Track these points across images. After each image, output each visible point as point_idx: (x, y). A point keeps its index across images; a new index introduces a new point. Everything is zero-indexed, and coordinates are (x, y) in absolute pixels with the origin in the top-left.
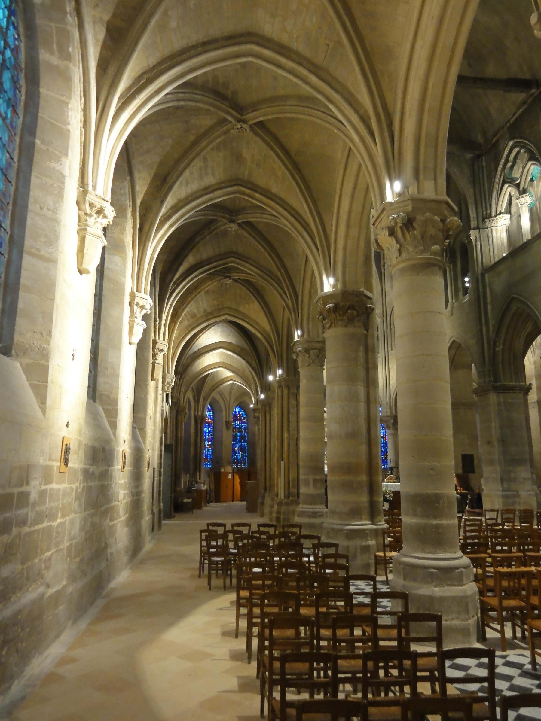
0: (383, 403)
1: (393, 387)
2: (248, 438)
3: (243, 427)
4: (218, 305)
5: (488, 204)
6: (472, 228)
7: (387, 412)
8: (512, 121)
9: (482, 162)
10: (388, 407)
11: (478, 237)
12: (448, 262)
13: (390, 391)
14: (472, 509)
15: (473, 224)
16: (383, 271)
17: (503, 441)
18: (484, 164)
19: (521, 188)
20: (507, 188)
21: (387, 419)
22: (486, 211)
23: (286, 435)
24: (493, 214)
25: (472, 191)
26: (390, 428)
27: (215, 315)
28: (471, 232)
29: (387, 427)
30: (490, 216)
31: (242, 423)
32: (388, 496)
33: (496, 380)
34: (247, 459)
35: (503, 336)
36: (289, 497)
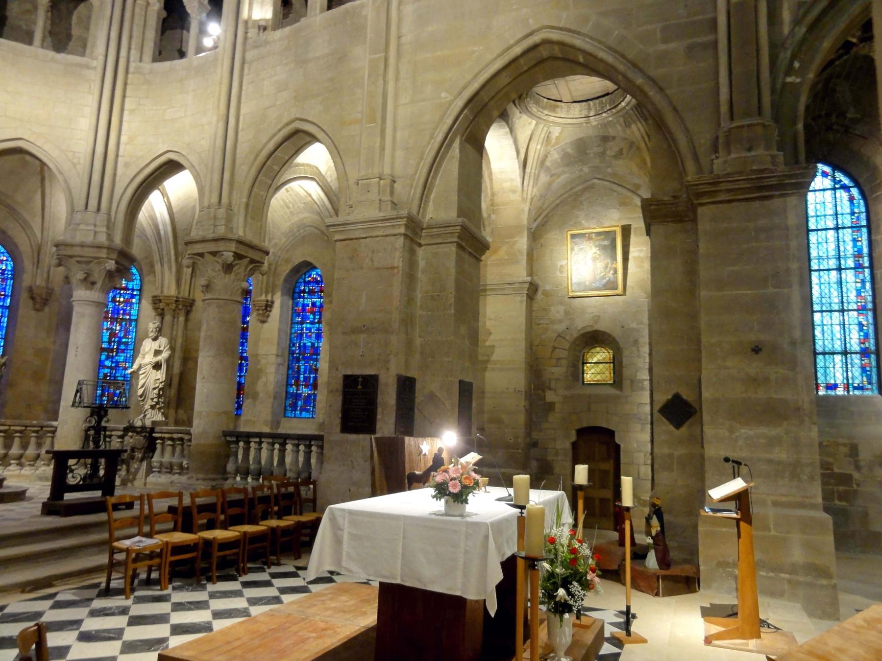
7: (95, 233)
10: (102, 217)
13: (115, 175)
21: (89, 253)
26: (93, 283)
29: (85, 279)
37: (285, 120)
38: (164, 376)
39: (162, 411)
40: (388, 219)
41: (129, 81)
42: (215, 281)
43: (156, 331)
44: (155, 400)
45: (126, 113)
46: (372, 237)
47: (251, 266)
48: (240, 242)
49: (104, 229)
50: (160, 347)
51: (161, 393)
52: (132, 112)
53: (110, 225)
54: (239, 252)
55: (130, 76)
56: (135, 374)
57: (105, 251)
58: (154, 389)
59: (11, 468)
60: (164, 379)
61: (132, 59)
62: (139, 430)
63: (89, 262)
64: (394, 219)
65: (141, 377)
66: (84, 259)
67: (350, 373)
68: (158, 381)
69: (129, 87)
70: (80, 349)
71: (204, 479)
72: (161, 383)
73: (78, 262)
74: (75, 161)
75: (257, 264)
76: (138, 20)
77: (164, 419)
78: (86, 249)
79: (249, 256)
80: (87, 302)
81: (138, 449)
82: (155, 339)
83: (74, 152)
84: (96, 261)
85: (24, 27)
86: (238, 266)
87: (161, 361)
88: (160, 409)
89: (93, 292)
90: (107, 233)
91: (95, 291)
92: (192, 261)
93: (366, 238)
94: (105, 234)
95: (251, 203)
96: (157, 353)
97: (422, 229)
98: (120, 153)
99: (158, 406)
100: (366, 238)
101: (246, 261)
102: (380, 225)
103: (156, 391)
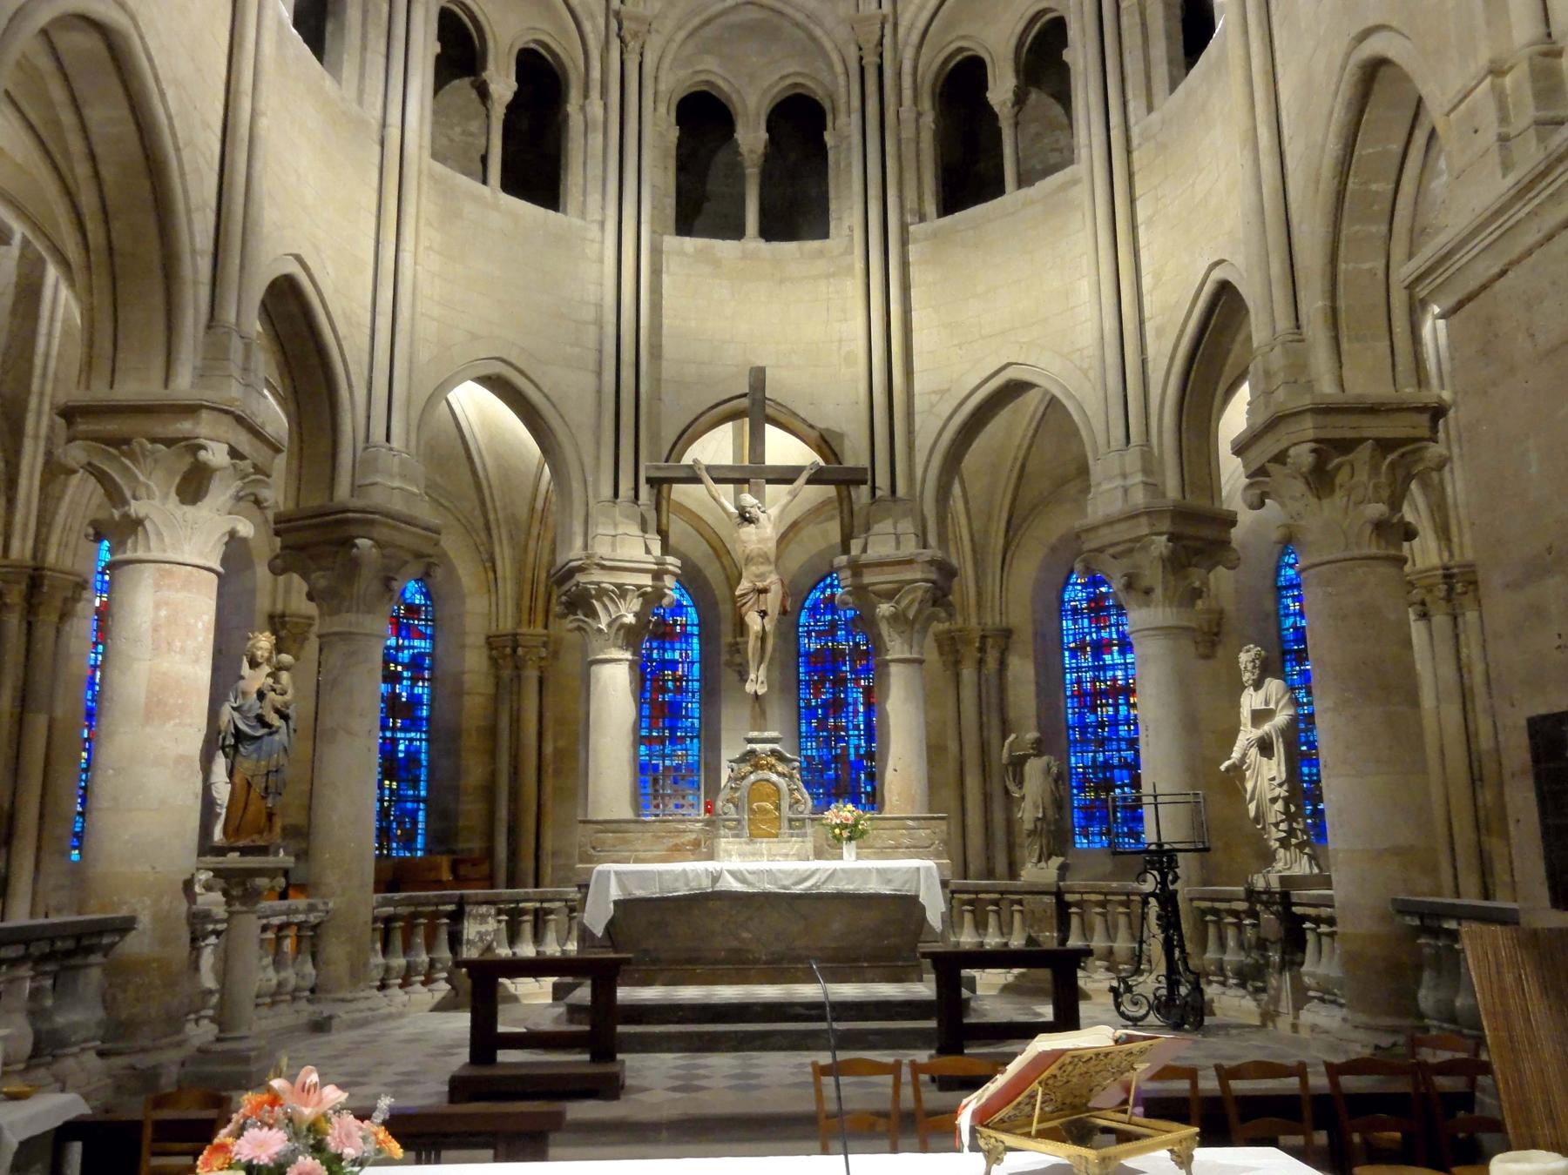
0: (1101, 439)
1: (1160, 332)
2: (431, 706)
3: (405, 656)
7: (1126, 490)
10: (1133, 458)
13: (1144, 362)
21: (1124, 532)
26: (1148, 592)
29: (1129, 587)
31: (398, 635)
34: (421, 816)
37: (1338, 63)
38: (1283, 768)
39: (1307, 850)
40: (1532, 184)
41: (1136, 166)
42: (1303, 523)
43: (1254, 667)
44: (1283, 826)
45: (1141, 230)
46: (1518, 261)
47: (1390, 458)
48: (1325, 410)
49: (1139, 478)
50: (1267, 703)
51: (1293, 809)
52: (1150, 221)
53: (1149, 465)
54: (1322, 434)
55: (1135, 155)
56: (1238, 770)
57: (1144, 520)
58: (1274, 800)
59: (1096, 976)
60: (1284, 776)
61: (1132, 120)
62: (1264, 897)
63: (1131, 551)
64: (1543, 175)
65: (1248, 773)
66: (1119, 548)
67: (1542, 711)
68: (1275, 783)
69: (1137, 178)
70: (1150, 729)
71: (1367, 1028)
72: (1280, 785)
73: (1114, 557)
74: (1086, 366)
75: (1403, 450)
76: (1132, 39)
77: (1316, 871)
78: (1117, 527)
79: (1365, 434)
80: (1146, 633)
81: (1272, 943)
82: (1258, 685)
83: (1080, 350)
84: (1138, 545)
85: (1039, 167)
86: (1346, 471)
87: (1269, 735)
88: (1301, 846)
89: (1152, 610)
90: (1145, 484)
91: (1156, 606)
92: (1258, 492)
93: (1503, 273)
94: (1141, 486)
95: (1342, 304)
96: (1259, 717)
98: (1147, 314)
99: (1294, 841)
100: (1503, 273)
101: (1364, 453)
102: (1522, 214)
103: (1279, 806)
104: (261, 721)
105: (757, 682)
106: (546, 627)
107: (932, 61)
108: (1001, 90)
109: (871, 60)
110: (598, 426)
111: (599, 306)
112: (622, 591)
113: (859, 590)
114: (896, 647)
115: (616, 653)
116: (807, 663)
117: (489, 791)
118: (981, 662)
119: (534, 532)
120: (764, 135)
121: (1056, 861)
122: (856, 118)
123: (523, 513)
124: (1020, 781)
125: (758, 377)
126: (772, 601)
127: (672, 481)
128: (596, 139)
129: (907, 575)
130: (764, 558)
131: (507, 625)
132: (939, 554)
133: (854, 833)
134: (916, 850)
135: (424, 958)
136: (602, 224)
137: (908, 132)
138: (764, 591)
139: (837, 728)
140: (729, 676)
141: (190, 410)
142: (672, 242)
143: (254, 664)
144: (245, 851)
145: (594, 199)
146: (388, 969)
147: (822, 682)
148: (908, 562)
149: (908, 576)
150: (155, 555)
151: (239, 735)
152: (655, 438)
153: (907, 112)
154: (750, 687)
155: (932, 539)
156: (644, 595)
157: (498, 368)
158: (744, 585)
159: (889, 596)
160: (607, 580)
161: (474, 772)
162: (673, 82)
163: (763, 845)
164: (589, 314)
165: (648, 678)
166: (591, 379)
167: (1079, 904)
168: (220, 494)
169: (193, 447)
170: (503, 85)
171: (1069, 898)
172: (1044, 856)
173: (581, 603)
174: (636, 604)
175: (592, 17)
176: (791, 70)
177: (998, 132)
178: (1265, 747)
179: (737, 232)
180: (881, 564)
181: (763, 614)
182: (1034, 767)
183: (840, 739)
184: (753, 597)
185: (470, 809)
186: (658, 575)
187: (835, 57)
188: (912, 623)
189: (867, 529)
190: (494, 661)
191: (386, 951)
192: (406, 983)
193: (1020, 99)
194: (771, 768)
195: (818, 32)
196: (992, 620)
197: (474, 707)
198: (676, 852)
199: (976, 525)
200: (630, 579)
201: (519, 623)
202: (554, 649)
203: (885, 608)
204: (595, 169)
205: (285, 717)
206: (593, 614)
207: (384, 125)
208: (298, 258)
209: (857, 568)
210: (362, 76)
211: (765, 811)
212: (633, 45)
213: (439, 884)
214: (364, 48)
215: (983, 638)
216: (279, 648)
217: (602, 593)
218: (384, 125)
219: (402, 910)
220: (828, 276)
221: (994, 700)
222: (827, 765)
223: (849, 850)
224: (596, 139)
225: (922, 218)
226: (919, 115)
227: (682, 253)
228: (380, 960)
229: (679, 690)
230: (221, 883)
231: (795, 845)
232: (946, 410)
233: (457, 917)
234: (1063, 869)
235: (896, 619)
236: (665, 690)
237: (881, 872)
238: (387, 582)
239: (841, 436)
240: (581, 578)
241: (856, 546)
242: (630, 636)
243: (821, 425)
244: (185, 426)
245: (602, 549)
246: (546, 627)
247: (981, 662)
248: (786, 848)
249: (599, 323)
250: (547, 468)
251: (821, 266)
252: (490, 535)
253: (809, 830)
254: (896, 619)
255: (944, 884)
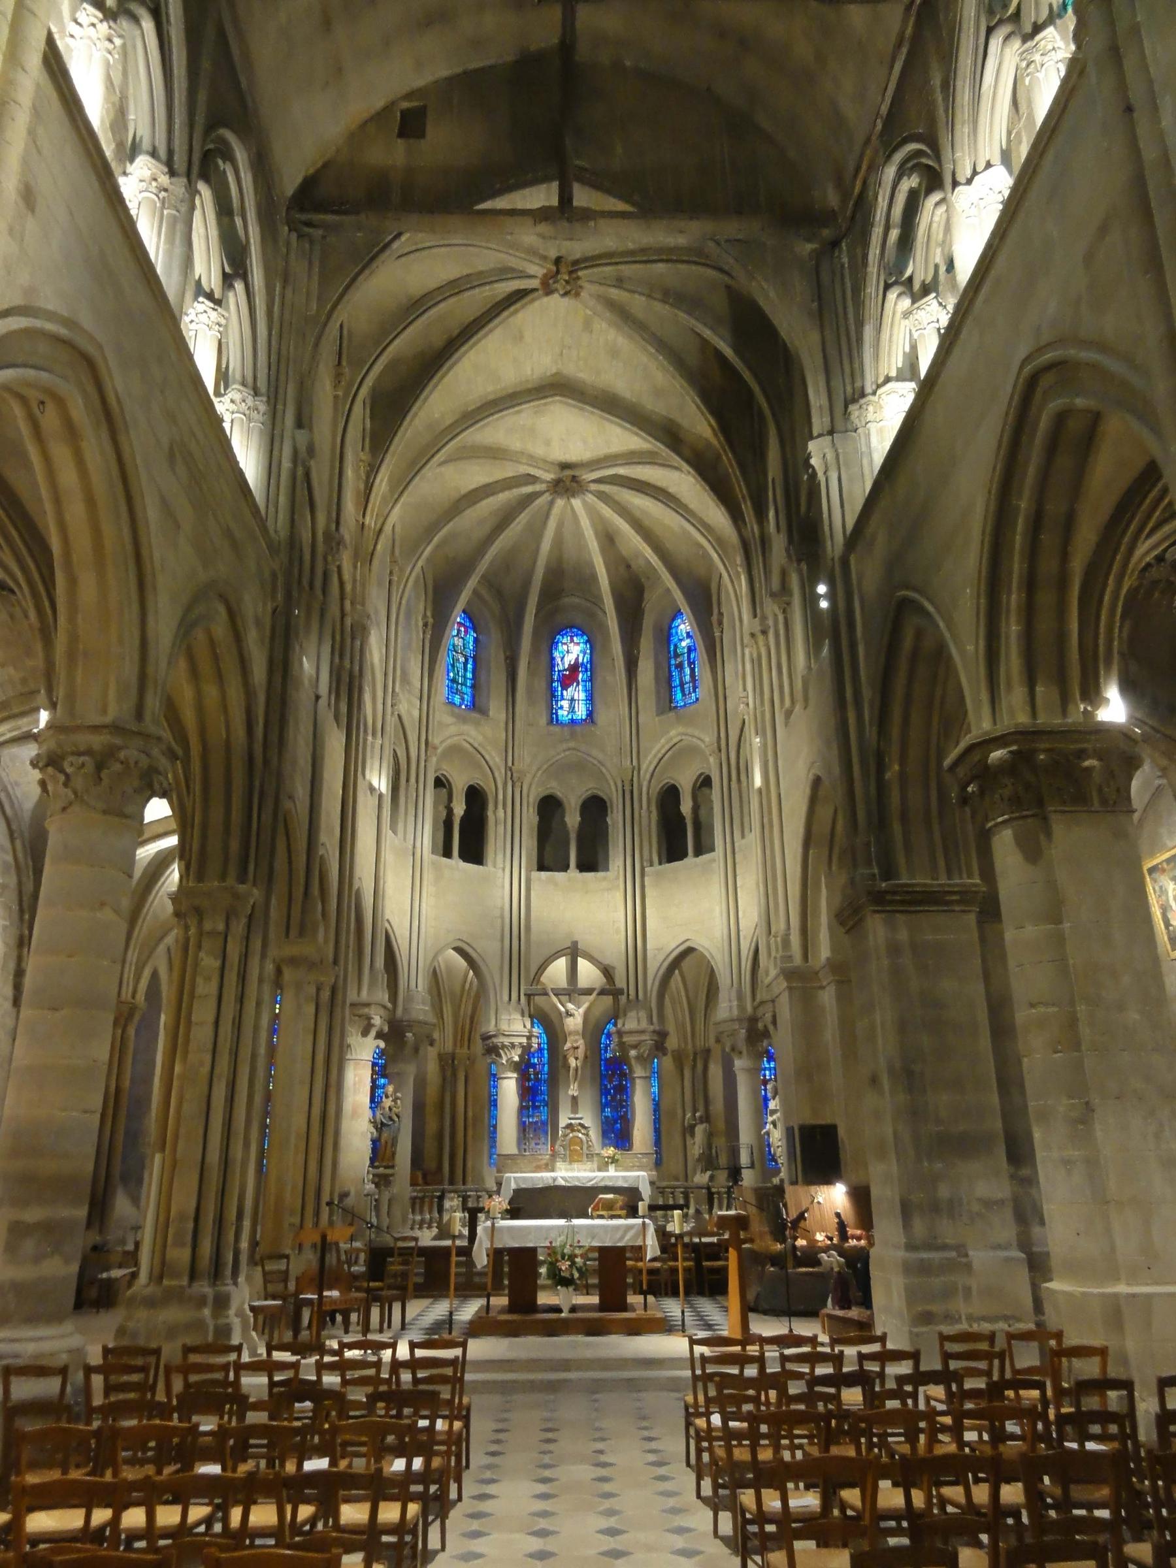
4: (24, 681)
5: (856, 366)
6: (815, 433)
7: (731, 1007)
8: (884, 109)
9: (839, 257)
10: (734, 994)
11: (830, 456)
12: (794, 558)
14: (842, 1308)
15: (819, 423)
16: (717, 634)
17: (910, 1074)
18: (845, 260)
19: (917, 286)
20: (896, 304)
22: (853, 382)
23: (178, 1069)
24: (868, 390)
25: (815, 337)
26: (740, 1053)
27: (16, 710)
28: (812, 446)
29: (733, 1049)
30: (863, 395)
32: (564, 1266)
33: (889, 872)
35: (895, 732)
36: (161, 1277)
41: (737, 860)
53: (740, 997)
56: (768, 1133)
97: (817, 973)
104: (391, 1119)
105: (573, 1090)
106: (469, 1048)
107: (656, 788)
108: (686, 807)
109: (627, 788)
110: (502, 968)
111: (502, 909)
112: (513, 1046)
113: (622, 1046)
114: (639, 1071)
115: (510, 1074)
116: (606, 1066)
117: (440, 1136)
118: (694, 1067)
119: (464, 1000)
120: (579, 819)
121: (709, 1173)
122: (621, 814)
123: (458, 989)
124: (693, 1135)
125: (575, 944)
126: (581, 1053)
127: (534, 995)
128: (501, 829)
129: (643, 1037)
130: (576, 1033)
131: (449, 1047)
132: (657, 1028)
133: (614, 1160)
134: (640, 1168)
135: (428, 1216)
136: (504, 869)
137: (645, 822)
138: (577, 1048)
139: (621, 1100)
140: (562, 1071)
141: (368, 1005)
142: (536, 875)
143: (387, 1097)
144: (386, 1167)
145: (500, 857)
146: (414, 1221)
147: (613, 1075)
148: (642, 1032)
149: (643, 1037)
150: (354, 1057)
151: (382, 1123)
152: (528, 970)
153: (644, 812)
154: (570, 1093)
155: (655, 1019)
156: (523, 1047)
157: (460, 944)
158: (568, 1045)
159: (635, 1047)
160: (506, 1041)
161: (431, 1126)
162: (534, 794)
163: (575, 1165)
164: (497, 913)
165: (529, 1094)
166: (497, 945)
167: (718, 1193)
168: (373, 1033)
169: (369, 1018)
170: (459, 809)
171: (714, 1190)
172: (704, 1171)
173: (493, 1050)
174: (519, 1051)
175: (499, 769)
176: (591, 786)
177: (685, 825)
178: (774, 1124)
179: (565, 868)
180: (631, 1032)
181: (576, 1059)
182: (700, 1130)
183: (623, 1107)
184: (571, 1052)
185: (430, 1146)
186: (529, 1038)
187: (612, 784)
188: (645, 1060)
189: (625, 1015)
190: (443, 1069)
191: (413, 1212)
192: (420, 1228)
193: (696, 809)
194: (579, 1131)
195: (604, 770)
196: (700, 1043)
197: (432, 1091)
198: (538, 1169)
199: (691, 994)
200: (517, 1040)
201: (455, 1044)
202: (471, 1059)
203: (633, 1053)
204: (500, 843)
205: (398, 1117)
206: (499, 1056)
207: (414, 847)
208: (388, 921)
209: (620, 1033)
210: (405, 826)
211: (576, 1151)
212: (518, 784)
213: (417, 1185)
214: (406, 814)
215: (695, 1054)
216: (395, 1091)
217: (504, 1047)
218: (414, 847)
219: (420, 1195)
220: (608, 890)
221: (701, 1087)
222: (616, 1122)
223: (612, 1168)
224: (501, 829)
225: (651, 865)
226: (650, 812)
227: (540, 879)
228: (411, 1216)
229: (537, 1080)
230: (377, 1180)
231: (589, 1165)
232: (661, 957)
233: (441, 1199)
234: (712, 1178)
235: (638, 1058)
236: (529, 1080)
237: (624, 1178)
238: (416, 1050)
239: (614, 968)
240: (495, 1040)
241: (620, 1023)
242: (516, 1067)
243: (606, 962)
244: (366, 1010)
245: (504, 1026)
246: (469, 1048)
247: (694, 1067)
248: (584, 1167)
249: (502, 917)
250: (471, 972)
251: (604, 884)
252: (441, 1001)
253: (595, 1159)
254: (639, 1058)
255: (652, 1183)
